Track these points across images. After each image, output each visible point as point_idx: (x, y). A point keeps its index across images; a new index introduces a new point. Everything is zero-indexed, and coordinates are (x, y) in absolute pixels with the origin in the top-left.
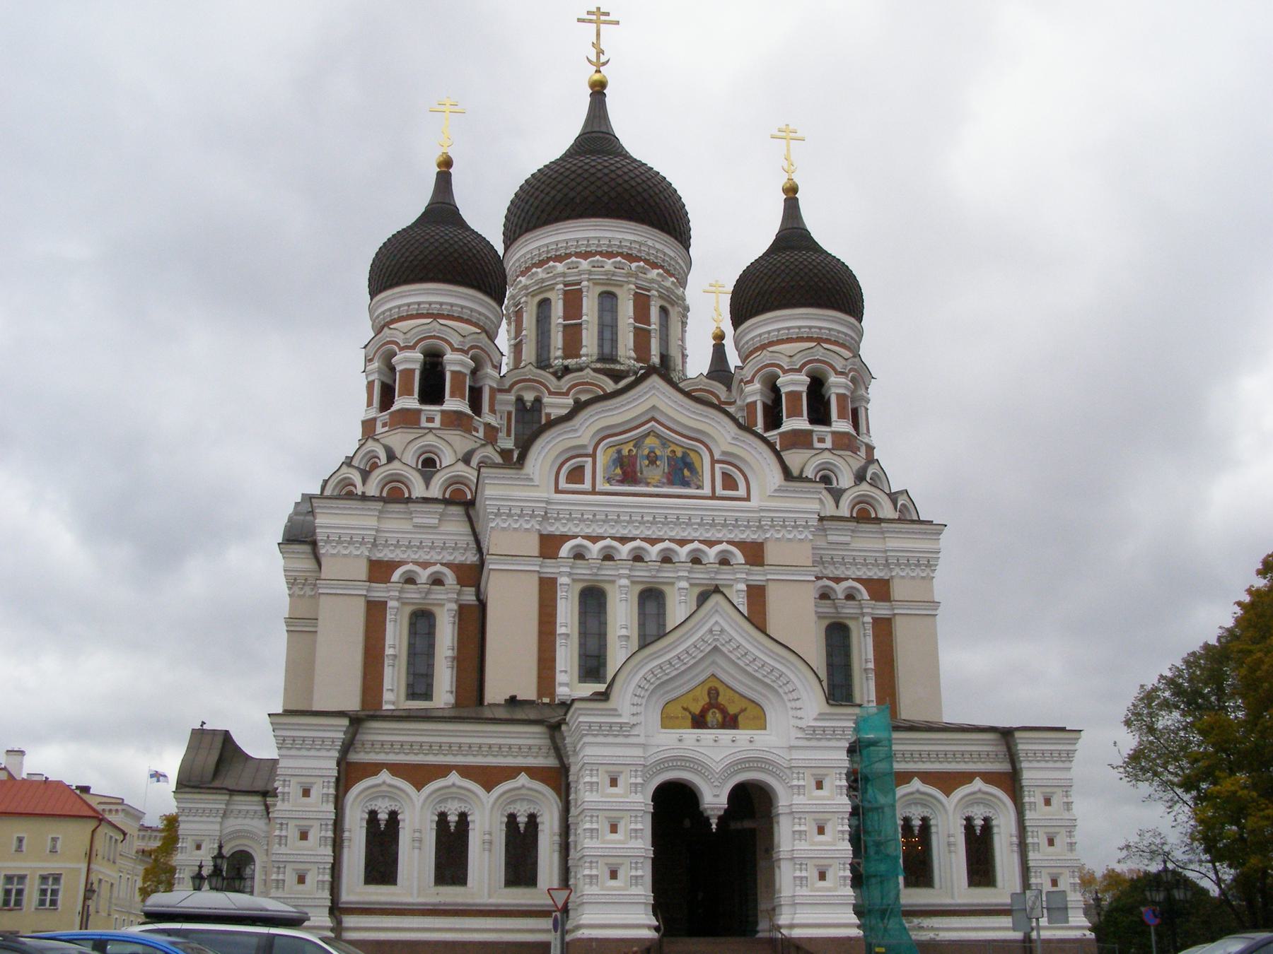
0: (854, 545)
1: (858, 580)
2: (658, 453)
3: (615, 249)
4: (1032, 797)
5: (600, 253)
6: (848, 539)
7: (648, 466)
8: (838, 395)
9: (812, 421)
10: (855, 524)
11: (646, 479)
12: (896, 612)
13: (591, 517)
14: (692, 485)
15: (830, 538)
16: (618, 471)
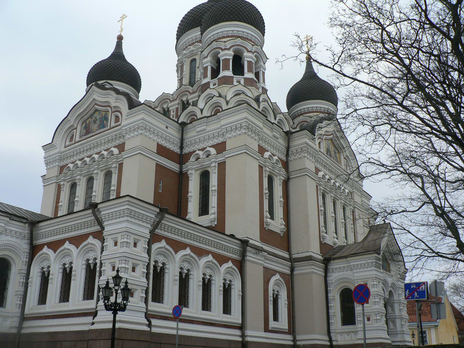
0: (208, 129)
1: (212, 146)
2: (97, 117)
3: (194, 41)
4: (109, 243)
5: (189, 45)
6: (205, 127)
7: (93, 125)
8: (223, 60)
9: (212, 78)
10: (206, 118)
11: (92, 130)
12: (226, 156)
13: (72, 154)
14: (106, 126)
15: (197, 130)
16: (85, 131)
